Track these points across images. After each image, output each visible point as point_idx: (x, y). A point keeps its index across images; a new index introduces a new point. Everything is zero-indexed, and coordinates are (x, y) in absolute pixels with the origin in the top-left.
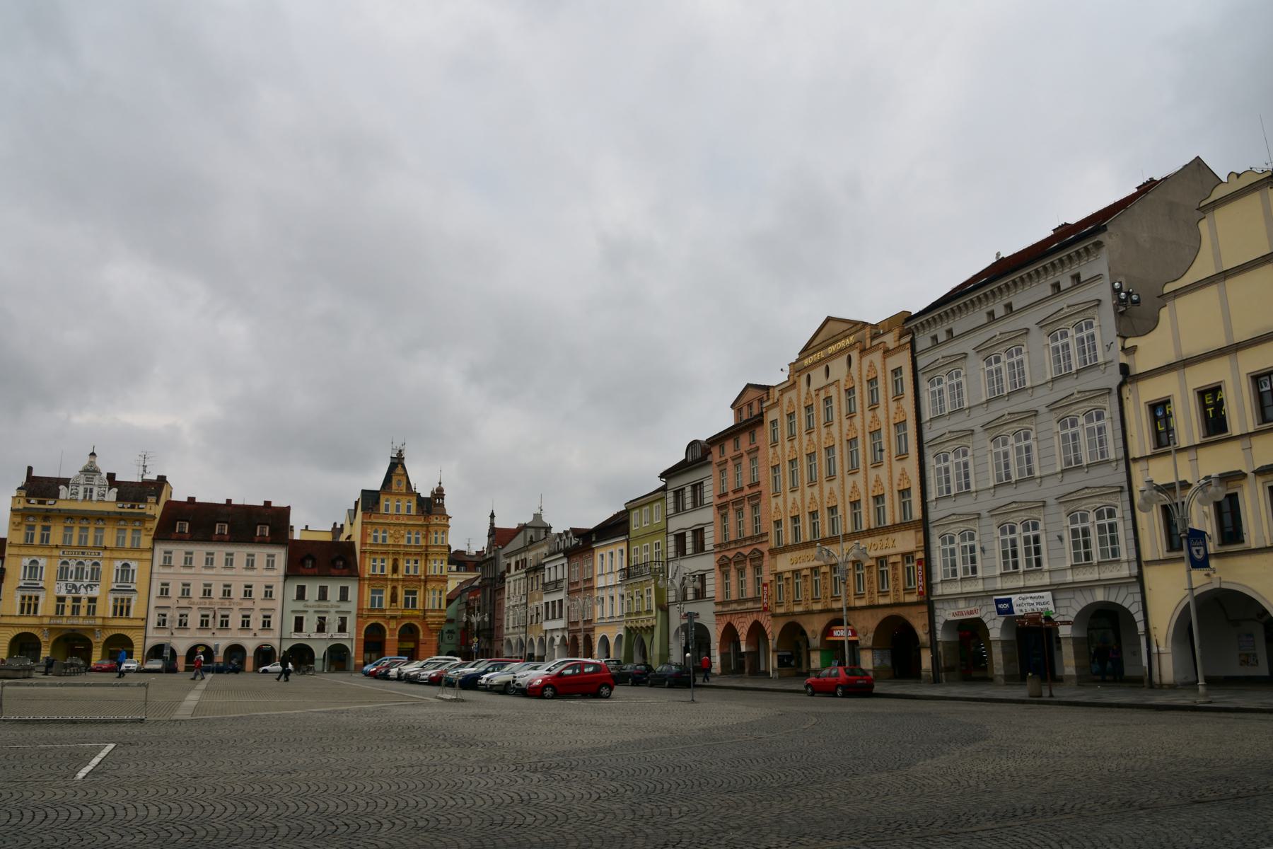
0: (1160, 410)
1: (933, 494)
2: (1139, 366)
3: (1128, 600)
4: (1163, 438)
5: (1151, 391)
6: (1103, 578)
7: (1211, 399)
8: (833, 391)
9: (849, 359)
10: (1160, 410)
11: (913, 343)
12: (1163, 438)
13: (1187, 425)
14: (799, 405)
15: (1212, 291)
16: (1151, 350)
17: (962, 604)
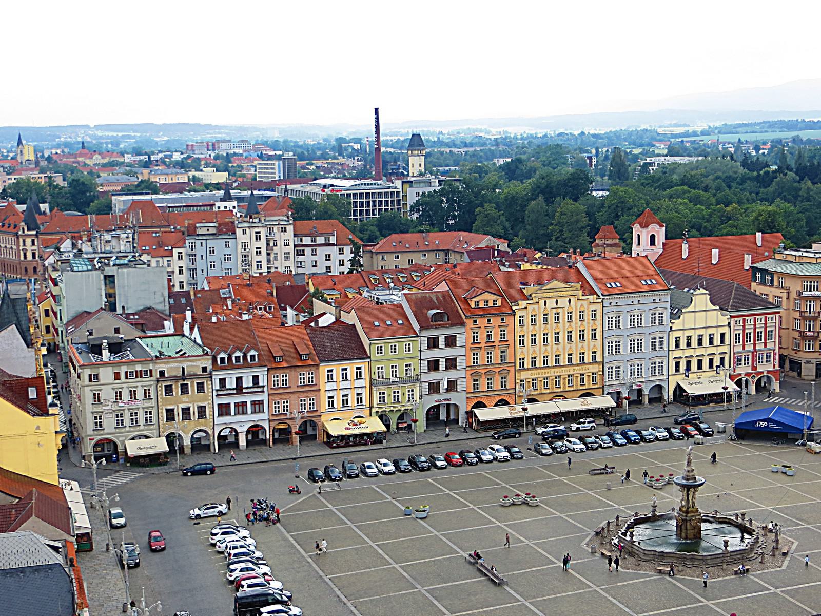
0: (677, 340)
1: (606, 354)
2: (674, 329)
3: (664, 384)
4: (677, 346)
5: (676, 334)
6: (657, 379)
7: (689, 339)
8: (560, 311)
9: (570, 301)
10: (677, 340)
11: (602, 302)
12: (677, 346)
13: (683, 344)
14: (540, 313)
15: (693, 314)
16: (677, 324)
17: (614, 387)
